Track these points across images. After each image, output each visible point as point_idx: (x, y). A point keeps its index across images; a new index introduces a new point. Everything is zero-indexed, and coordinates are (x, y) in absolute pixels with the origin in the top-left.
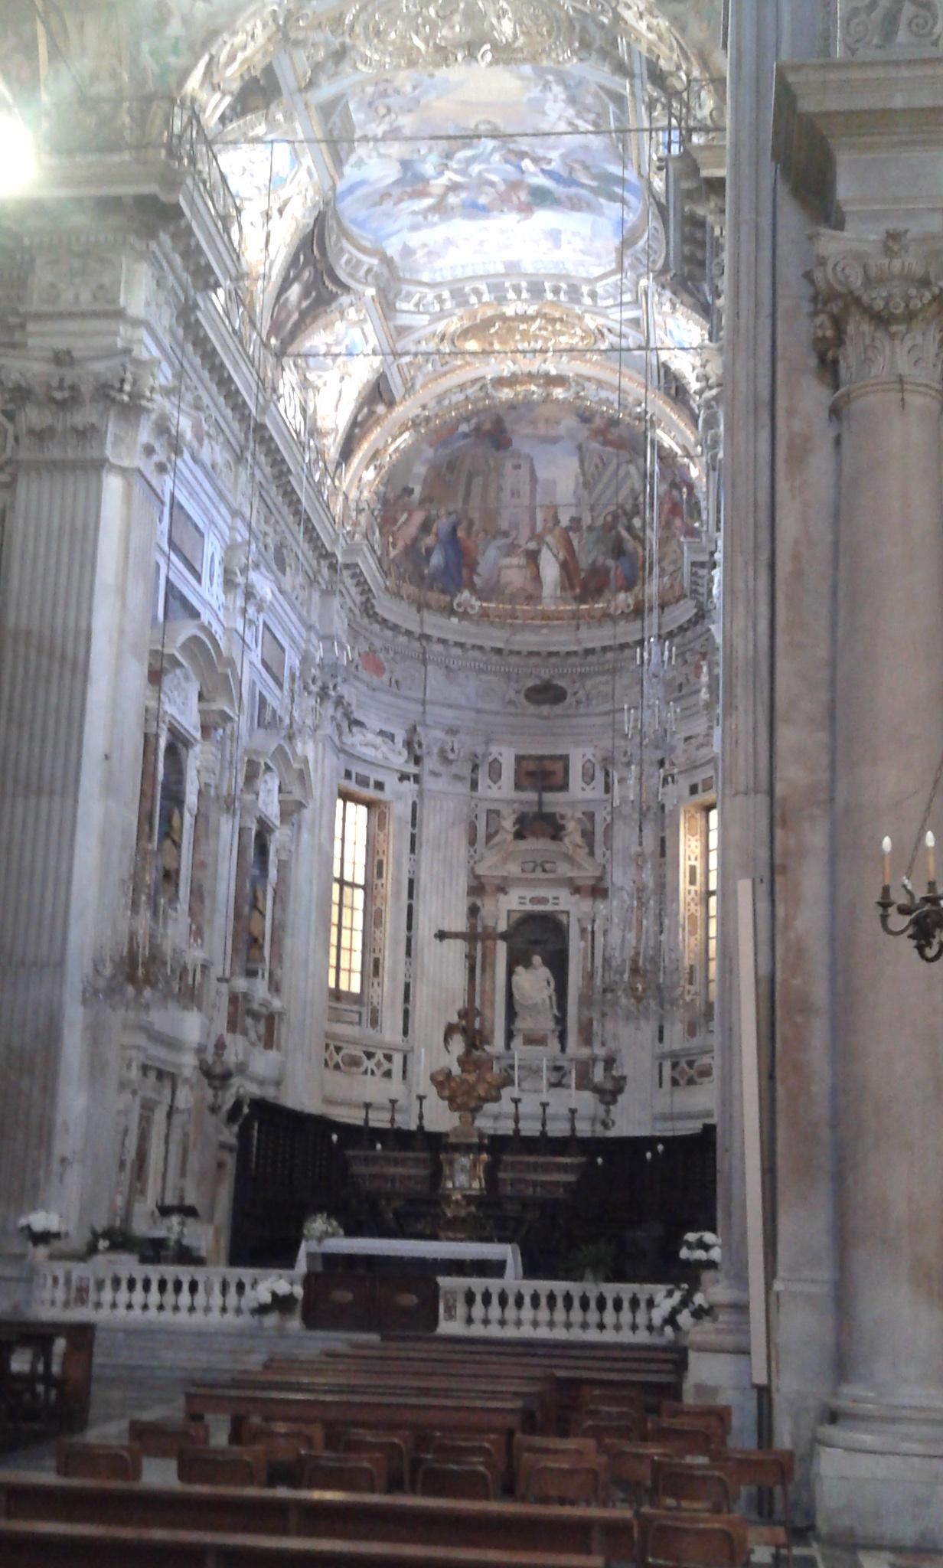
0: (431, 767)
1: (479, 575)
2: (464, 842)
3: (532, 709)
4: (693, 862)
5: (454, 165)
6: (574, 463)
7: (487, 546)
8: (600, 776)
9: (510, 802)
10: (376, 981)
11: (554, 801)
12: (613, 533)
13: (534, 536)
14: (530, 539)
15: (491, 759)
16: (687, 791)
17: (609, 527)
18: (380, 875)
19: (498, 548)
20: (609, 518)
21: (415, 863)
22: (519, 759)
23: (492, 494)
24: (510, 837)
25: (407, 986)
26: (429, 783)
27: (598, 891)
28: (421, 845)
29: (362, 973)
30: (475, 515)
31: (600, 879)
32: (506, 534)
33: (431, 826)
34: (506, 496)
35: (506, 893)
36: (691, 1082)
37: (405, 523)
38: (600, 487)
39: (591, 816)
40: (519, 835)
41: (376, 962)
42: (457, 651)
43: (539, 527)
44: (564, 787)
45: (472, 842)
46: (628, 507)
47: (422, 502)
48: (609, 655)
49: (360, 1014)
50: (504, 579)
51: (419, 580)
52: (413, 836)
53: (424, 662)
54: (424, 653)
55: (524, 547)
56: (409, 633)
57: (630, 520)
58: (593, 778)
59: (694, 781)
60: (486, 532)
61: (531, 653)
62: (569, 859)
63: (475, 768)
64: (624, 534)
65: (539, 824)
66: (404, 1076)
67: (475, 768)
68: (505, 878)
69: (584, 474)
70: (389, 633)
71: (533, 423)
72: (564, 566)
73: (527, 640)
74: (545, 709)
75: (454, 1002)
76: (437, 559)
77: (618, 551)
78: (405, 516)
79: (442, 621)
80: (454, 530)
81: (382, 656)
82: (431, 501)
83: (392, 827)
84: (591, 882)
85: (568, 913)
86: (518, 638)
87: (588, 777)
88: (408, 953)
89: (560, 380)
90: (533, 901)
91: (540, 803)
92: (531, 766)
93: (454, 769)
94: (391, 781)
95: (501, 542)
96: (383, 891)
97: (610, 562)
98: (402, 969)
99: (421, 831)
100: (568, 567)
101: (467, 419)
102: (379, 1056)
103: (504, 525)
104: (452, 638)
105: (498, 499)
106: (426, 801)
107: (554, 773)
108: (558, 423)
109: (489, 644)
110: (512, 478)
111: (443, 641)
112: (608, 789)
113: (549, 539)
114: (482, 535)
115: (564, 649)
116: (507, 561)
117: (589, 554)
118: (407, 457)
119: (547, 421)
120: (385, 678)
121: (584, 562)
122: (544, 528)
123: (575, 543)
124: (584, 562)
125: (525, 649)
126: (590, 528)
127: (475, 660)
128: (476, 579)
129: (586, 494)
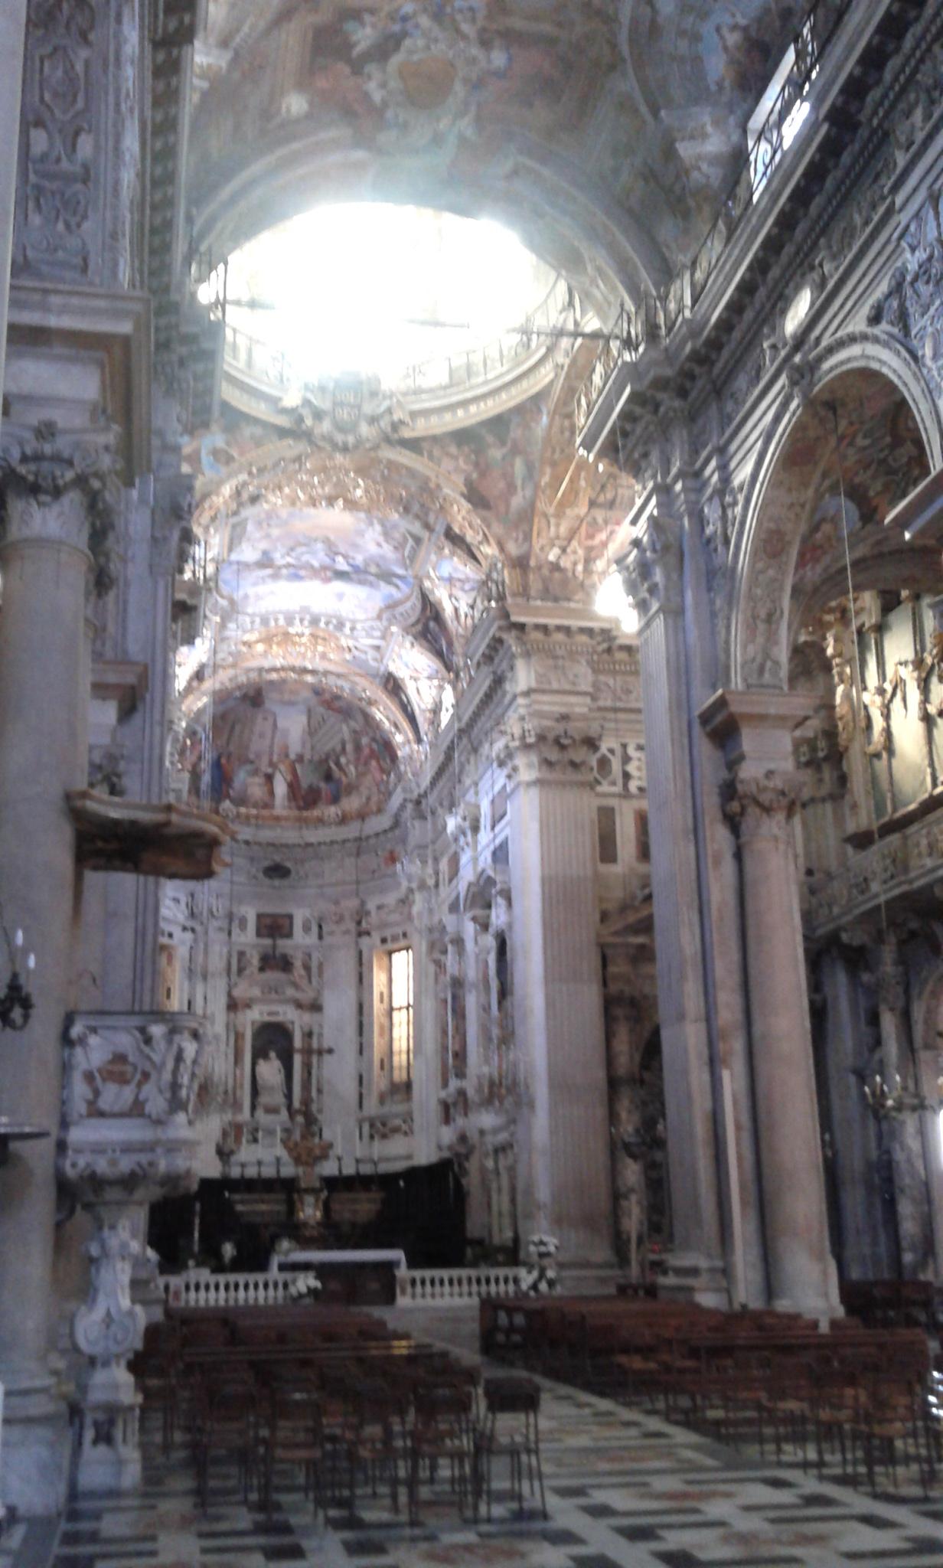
3: (267, 881)
5: (293, 554)
6: (304, 719)
8: (315, 929)
9: (254, 946)
11: (284, 945)
13: (271, 764)
16: (378, 942)
22: (259, 916)
24: (256, 971)
27: (316, 1007)
32: (252, 762)
34: (255, 738)
36: (384, 1136)
39: (309, 956)
40: (262, 969)
44: (289, 935)
46: (339, 748)
62: (296, 986)
63: (230, 923)
65: (276, 962)
73: (267, 835)
74: (277, 882)
77: (328, 777)
87: (307, 929)
89: (313, 672)
90: (270, 1014)
91: (274, 947)
92: (268, 921)
95: (249, 767)
97: (323, 785)
100: (293, 787)
103: (252, 756)
110: (261, 725)
112: (320, 937)
113: (282, 767)
115: (290, 842)
123: (299, 771)
126: (310, 761)
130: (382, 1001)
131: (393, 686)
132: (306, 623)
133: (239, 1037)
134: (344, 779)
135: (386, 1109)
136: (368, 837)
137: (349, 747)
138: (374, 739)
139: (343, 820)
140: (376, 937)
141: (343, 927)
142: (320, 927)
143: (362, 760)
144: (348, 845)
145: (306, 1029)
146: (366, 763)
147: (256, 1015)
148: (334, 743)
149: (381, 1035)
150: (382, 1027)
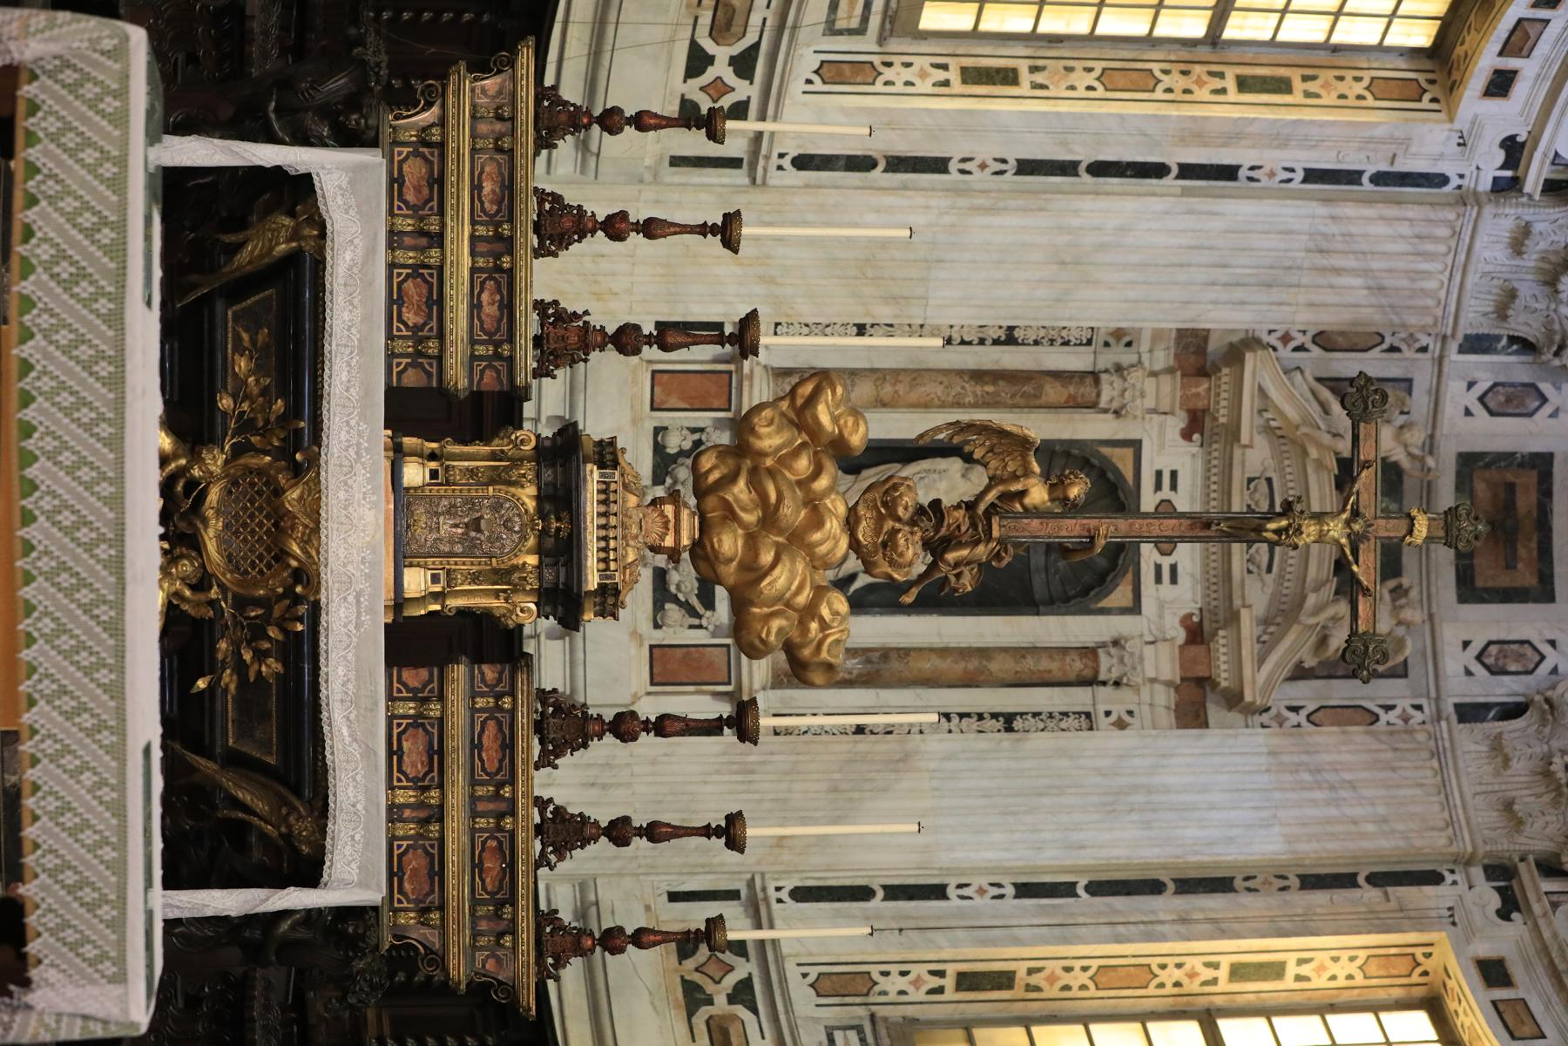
0: (1538, 227)
2: (1331, 319)
4: (1292, 970)
8: (1504, 689)
10: (953, 75)
15: (1546, 387)
18: (1244, 84)
21: (1283, 189)
25: (938, 165)
26: (1498, 223)
27: (1198, 699)
28: (1327, 200)
29: (975, 35)
31: (1234, 700)
33: (1380, 229)
35: (1187, 435)
36: (694, 997)
39: (1402, 672)
41: (1008, 77)
44: (1469, 590)
45: (1324, 340)
49: (861, 31)
52: (1353, 177)
58: (1496, 671)
59: (1516, 970)
62: (1283, 615)
63: (1525, 346)
66: (677, 161)
67: (1525, 346)
68: (1233, 432)
75: (893, 299)
83: (1381, 119)
84: (1224, 679)
85: (1135, 608)
87: (1497, 657)
88: (1027, 167)
92: (1526, 501)
93: (1528, 289)
94: (1509, 115)
96: (1203, 94)
98: (986, 150)
99: (1367, 201)
102: (743, 90)
106: (1450, 215)
107: (1510, 565)
112: (1469, 713)
130: (1238, 972)
133: (1080, 389)
135: (802, 998)
140: (1505, 940)
141: (1527, 801)
142: (1512, 711)
145: (1108, 666)
147: (1169, 462)
149: (1105, 975)
150: (1144, 973)
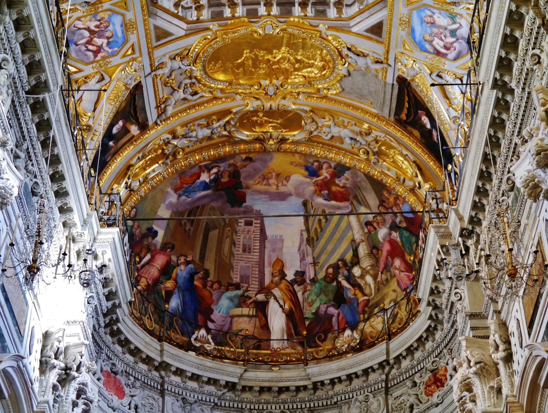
1: (213, 321)
7: (219, 298)
12: (335, 284)
13: (262, 289)
14: (259, 292)
17: (331, 278)
19: (231, 299)
20: (331, 270)
23: (226, 249)
30: (210, 265)
32: (237, 287)
34: (238, 251)
37: (148, 263)
38: (323, 241)
42: (193, 385)
43: (267, 281)
46: (349, 257)
47: (165, 246)
48: (339, 388)
50: (235, 328)
51: (160, 313)
53: (162, 393)
54: (162, 385)
55: (254, 299)
56: (148, 360)
57: (349, 270)
60: (219, 283)
61: (262, 390)
64: (345, 283)
69: (308, 230)
70: (129, 358)
71: (265, 178)
72: (290, 316)
76: (174, 303)
77: (339, 298)
78: (148, 257)
79: (180, 353)
80: (191, 276)
81: (122, 379)
82: (173, 248)
86: (251, 374)
97: (332, 310)
100: (293, 317)
101: (208, 169)
103: (236, 279)
104: (190, 370)
105: (231, 254)
108: (288, 178)
109: (223, 378)
110: (244, 234)
111: (179, 372)
113: (276, 292)
114: (216, 286)
116: (238, 311)
117: (313, 303)
118: (157, 191)
119: (278, 175)
120: (126, 401)
121: (309, 312)
122: (272, 281)
123: (300, 294)
124: (309, 312)
125: (257, 385)
126: (314, 281)
127: (210, 395)
128: (210, 325)
129: (310, 250)
131: (409, 107)
132: (275, 10)
134: (362, 299)
136: (398, 359)
137: (363, 250)
138: (394, 227)
139: (364, 345)
143: (382, 266)
144: (373, 377)
146: (387, 268)
148: (342, 250)
